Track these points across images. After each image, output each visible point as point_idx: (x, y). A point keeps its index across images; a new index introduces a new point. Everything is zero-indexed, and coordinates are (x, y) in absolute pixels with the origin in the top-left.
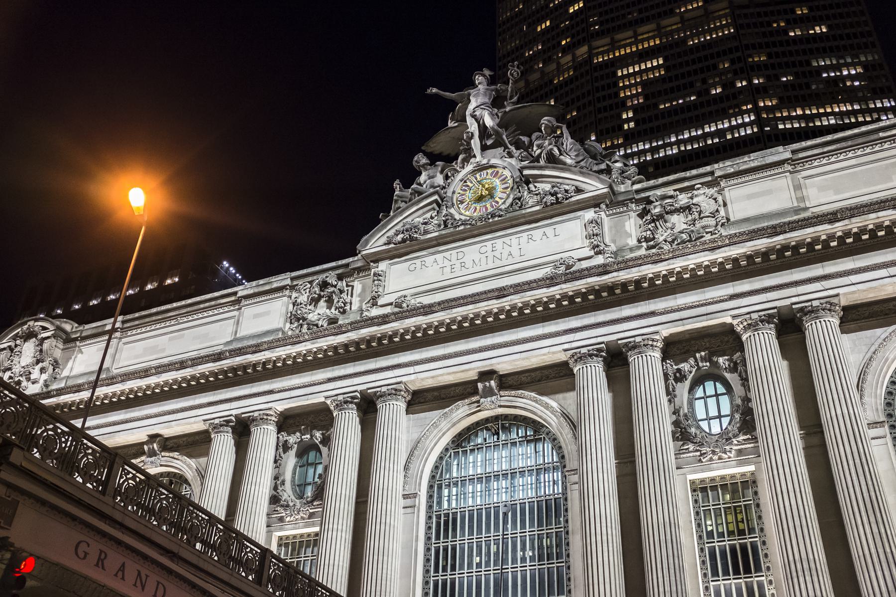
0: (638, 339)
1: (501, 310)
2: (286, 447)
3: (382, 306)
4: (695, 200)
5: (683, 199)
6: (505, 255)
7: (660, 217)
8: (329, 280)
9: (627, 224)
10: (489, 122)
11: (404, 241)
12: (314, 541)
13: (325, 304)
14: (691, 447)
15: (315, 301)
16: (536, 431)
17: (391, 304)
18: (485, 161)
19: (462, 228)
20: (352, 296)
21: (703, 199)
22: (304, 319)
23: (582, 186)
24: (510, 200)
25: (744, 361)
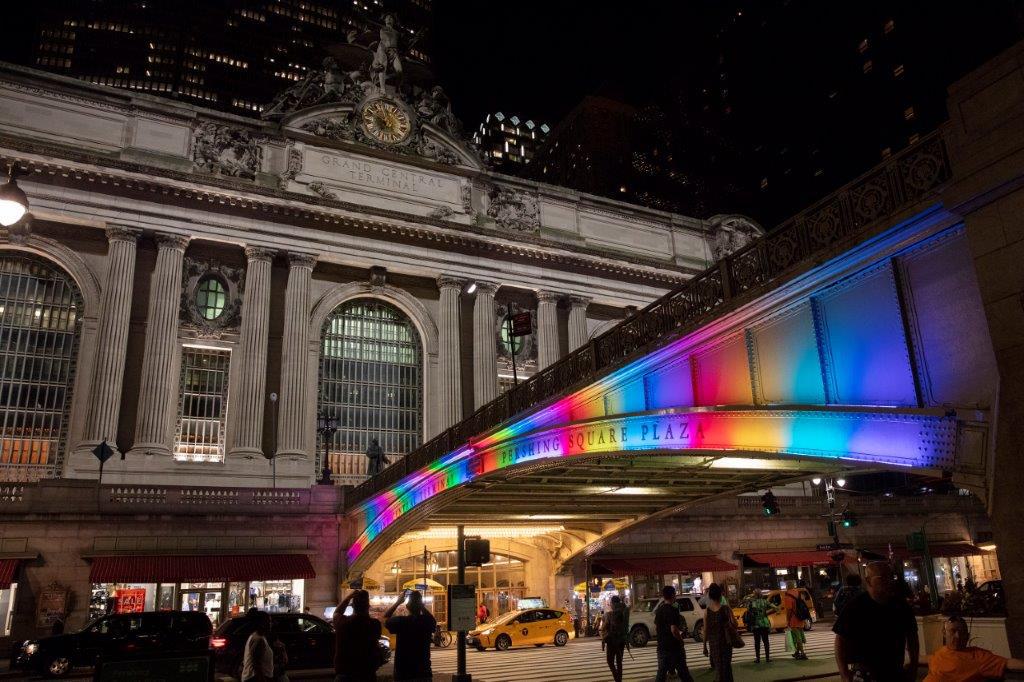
0: (489, 284)
1: (404, 229)
2: (193, 271)
3: (299, 182)
4: (523, 201)
5: (517, 197)
6: (402, 185)
7: (503, 203)
8: (242, 134)
9: (483, 198)
10: (397, 65)
11: (325, 135)
12: (222, 359)
13: (233, 154)
14: (504, 359)
15: (223, 146)
16: (400, 318)
17: (307, 184)
18: (390, 97)
19: (374, 148)
20: (261, 157)
21: (528, 200)
22: (214, 160)
23: (462, 158)
24: (408, 142)
25: (536, 315)
